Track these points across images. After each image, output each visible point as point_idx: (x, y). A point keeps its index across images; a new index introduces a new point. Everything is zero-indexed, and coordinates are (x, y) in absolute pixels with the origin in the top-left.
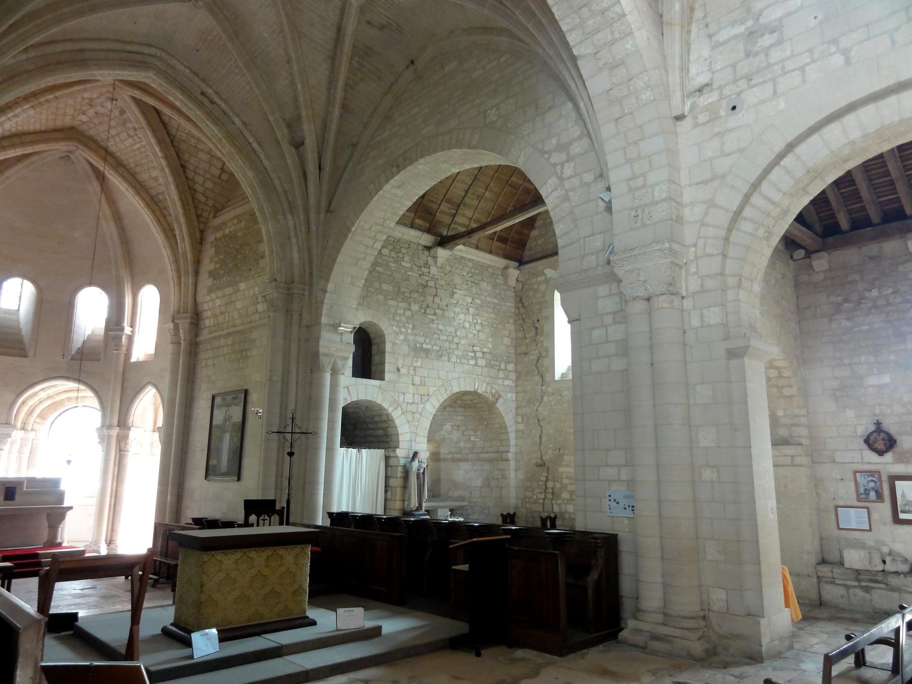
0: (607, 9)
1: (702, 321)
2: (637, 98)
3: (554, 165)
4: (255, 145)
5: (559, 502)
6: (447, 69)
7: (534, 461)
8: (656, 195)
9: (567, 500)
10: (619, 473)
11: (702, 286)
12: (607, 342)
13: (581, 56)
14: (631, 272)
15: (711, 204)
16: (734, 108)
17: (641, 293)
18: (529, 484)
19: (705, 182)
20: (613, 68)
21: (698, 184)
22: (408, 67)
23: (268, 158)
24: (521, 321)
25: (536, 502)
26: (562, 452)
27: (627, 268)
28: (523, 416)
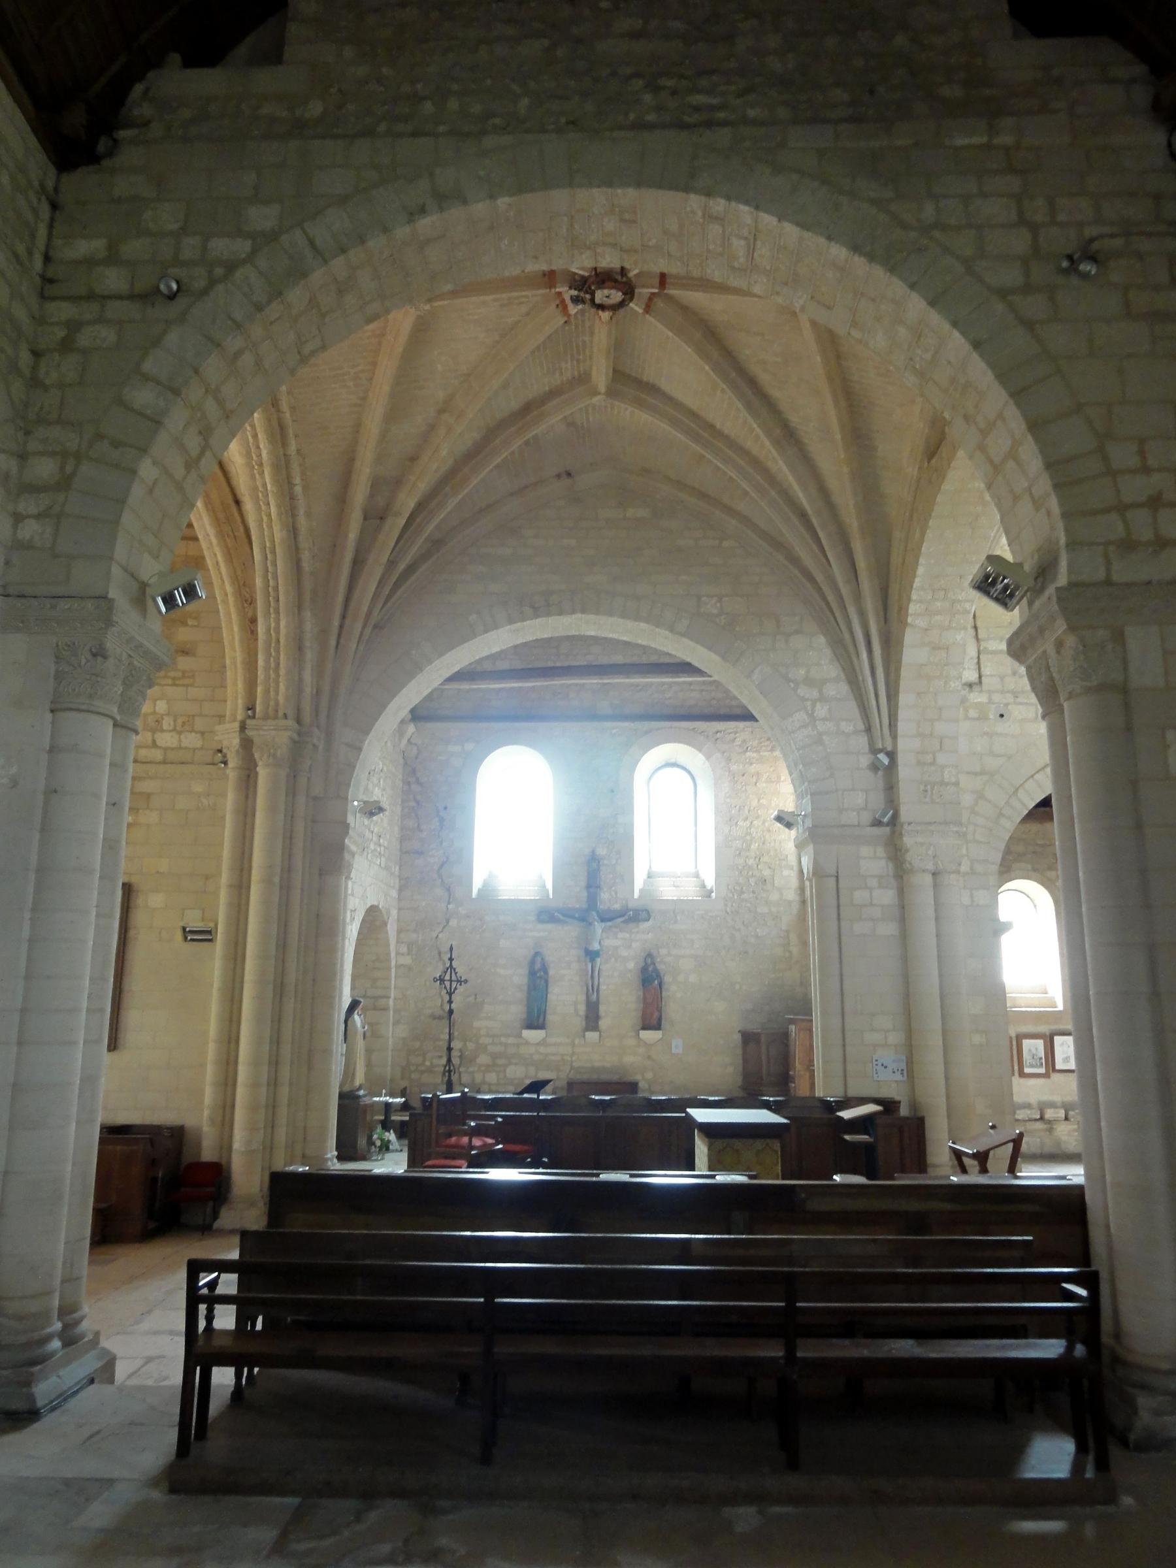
0: (959, 601)
1: (973, 901)
2: (946, 683)
3: (803, 699)
4: (298, 489)
5: (471, 1069)
6: (630, 512)
7: (429, 1012)
8: (946, 776)
9: (488, 1066)
10: (886, 1038)
11: (971, 868)
12: (871, 905)
13: (912, 626)
14: (922, 844)
15: (980, 796)
16: (1002, 716)
17: (930, 866)
18: (417, 1044)
19: (976, 774)
20: (936, 648)
21: (968, 773)
22: (559, 476)
23: (308, 515)
24: (413, 804)
25: (430, 1070)
26: (479, 1000)
27: (920, 839)
28: (410, 945)
